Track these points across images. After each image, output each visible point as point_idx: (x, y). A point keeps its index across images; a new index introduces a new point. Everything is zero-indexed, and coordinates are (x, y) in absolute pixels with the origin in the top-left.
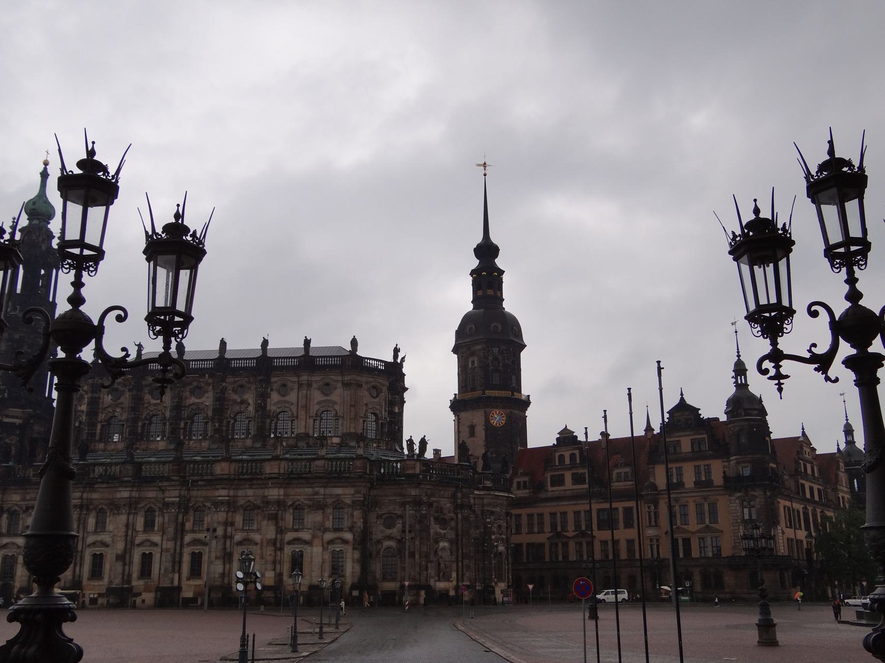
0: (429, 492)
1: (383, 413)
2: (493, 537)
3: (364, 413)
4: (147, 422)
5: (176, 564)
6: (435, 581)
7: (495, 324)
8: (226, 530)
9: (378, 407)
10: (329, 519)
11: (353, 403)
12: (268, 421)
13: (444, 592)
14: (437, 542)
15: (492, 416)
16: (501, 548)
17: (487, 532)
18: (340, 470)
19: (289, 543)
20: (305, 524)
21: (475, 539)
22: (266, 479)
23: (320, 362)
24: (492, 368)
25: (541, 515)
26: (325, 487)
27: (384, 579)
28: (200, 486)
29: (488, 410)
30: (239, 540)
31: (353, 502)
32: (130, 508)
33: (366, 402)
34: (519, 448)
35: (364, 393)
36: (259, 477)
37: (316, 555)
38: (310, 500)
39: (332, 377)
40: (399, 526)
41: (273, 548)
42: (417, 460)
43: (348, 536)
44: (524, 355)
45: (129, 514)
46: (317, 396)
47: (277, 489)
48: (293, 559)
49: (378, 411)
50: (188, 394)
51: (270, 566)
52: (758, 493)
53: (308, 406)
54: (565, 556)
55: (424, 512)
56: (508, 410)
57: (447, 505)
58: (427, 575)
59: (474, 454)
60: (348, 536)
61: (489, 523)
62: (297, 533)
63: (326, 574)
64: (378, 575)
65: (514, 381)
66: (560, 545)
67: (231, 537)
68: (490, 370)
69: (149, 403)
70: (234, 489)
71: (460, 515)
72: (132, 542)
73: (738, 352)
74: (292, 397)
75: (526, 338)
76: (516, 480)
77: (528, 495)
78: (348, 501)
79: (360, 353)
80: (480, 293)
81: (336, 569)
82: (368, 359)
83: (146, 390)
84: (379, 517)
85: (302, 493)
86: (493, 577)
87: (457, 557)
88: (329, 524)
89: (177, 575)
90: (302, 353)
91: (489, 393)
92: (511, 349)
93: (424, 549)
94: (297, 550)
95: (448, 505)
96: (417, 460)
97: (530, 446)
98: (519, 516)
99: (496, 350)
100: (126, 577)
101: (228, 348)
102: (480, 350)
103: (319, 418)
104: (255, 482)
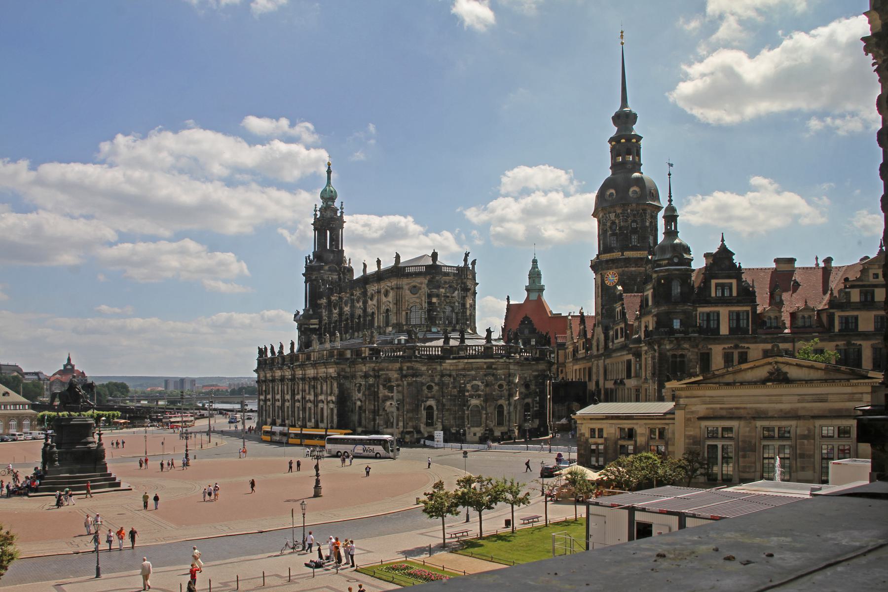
2: (467, 394)
5: (293, 412)
15: (606, 278)
17: (462, 391)
26: (326, 368)
29: (603, 272)
56: (621, 270)
57: (394, 375)
58: (375, 424)
60: (334, 398)
61: (463, 384)
67: (305, 398)
84: (356, 384)
85: (322, 371)
88: (329, 393)
95: (396, 376)
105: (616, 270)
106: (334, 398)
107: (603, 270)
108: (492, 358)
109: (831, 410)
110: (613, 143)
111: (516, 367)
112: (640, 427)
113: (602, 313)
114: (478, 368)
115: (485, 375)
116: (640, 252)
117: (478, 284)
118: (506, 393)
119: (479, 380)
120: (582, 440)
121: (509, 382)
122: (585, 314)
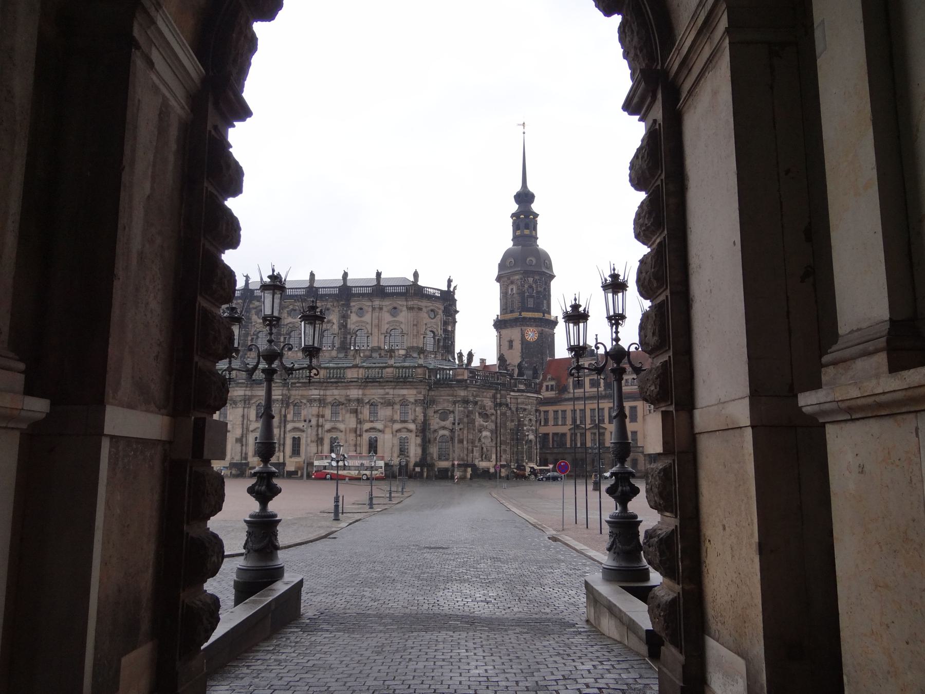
0: (475, 393)
1: (439, 330)
2: (525, 428)
3: (424, 330)
4: (255, 337)
6: (479, 461)
7: (531, 259)
8: (318, 421)
9: (435, 326)
10: (397, 412)
11: (415, 323)
12: (349, 337)
13: (486, 470)
14: (480, 431)
16: (531, 437)
17: (520, 424)
18: (405, 376)
19: (366, 431)
20: (379, 418)
21: (511, 430)
22: (348, 382)
23: (389, 290)
24: (527, 294)
25: (564, 412)
26: (394, 389)
27: (440, 459)
28: (300, 387)
30: (329, 428)
31: (416, 401)
32: (245, 403)
33: (425, 322)
34: (548, 358)
35: (424, 315)
36: (343, 380)
37: (387, 442)
38: (382, 398)
39: (399, 302)
40: (451, 419)
41: (355, 435)
42: (465, 369)
43: (412, 426)
44: (553, 283)
45: (244, 407)
46: (387, 317)
47: (357, 390)
48: (370, 444)
49: (436, 330)
50: (286, 314)
51: (353, 448)
53: (380, 325)
54: (584, 444)
55: (470, 409)
57: (488, 403)
58: (473, 456)
59: (513, 363)
61: (522, 417)
62: (372, 423)
63: (395, 455)
64: (435, 456)
65: (545, 305)
66: (579, 434)
67: (322, 426)
69: (256, 322)
70: (324, 390)
71: (499, 412)
72: (247, 429)
74: (367, 318)
75: (556, 270)
76: (545, 384)
77: (554, 396)
78: (412, 400)
79: (421, 283)
80: (518, 233)
81: (403, 451)
82: (427, 287)
83: (253, 311)
85: (375, 393)
86: (525, 458)
87: (496, 444)
88: (397, 417)
89: (282, 454)
90: (375, 283)
91: (524, 314)
93: (471, 437)
94: (373, 437)
95: (490, 403)
96: (465, 369)
97: (556, 358)
98: (546, 412)
99: (531, 280)
100: (243, 455)
101: (316, 278)
102: (518, 280)
103: (388, 335)
104: (340, 384)
106: (412, 426)
107: (522, 325)
110: (514, 218)
114: (532, 404)
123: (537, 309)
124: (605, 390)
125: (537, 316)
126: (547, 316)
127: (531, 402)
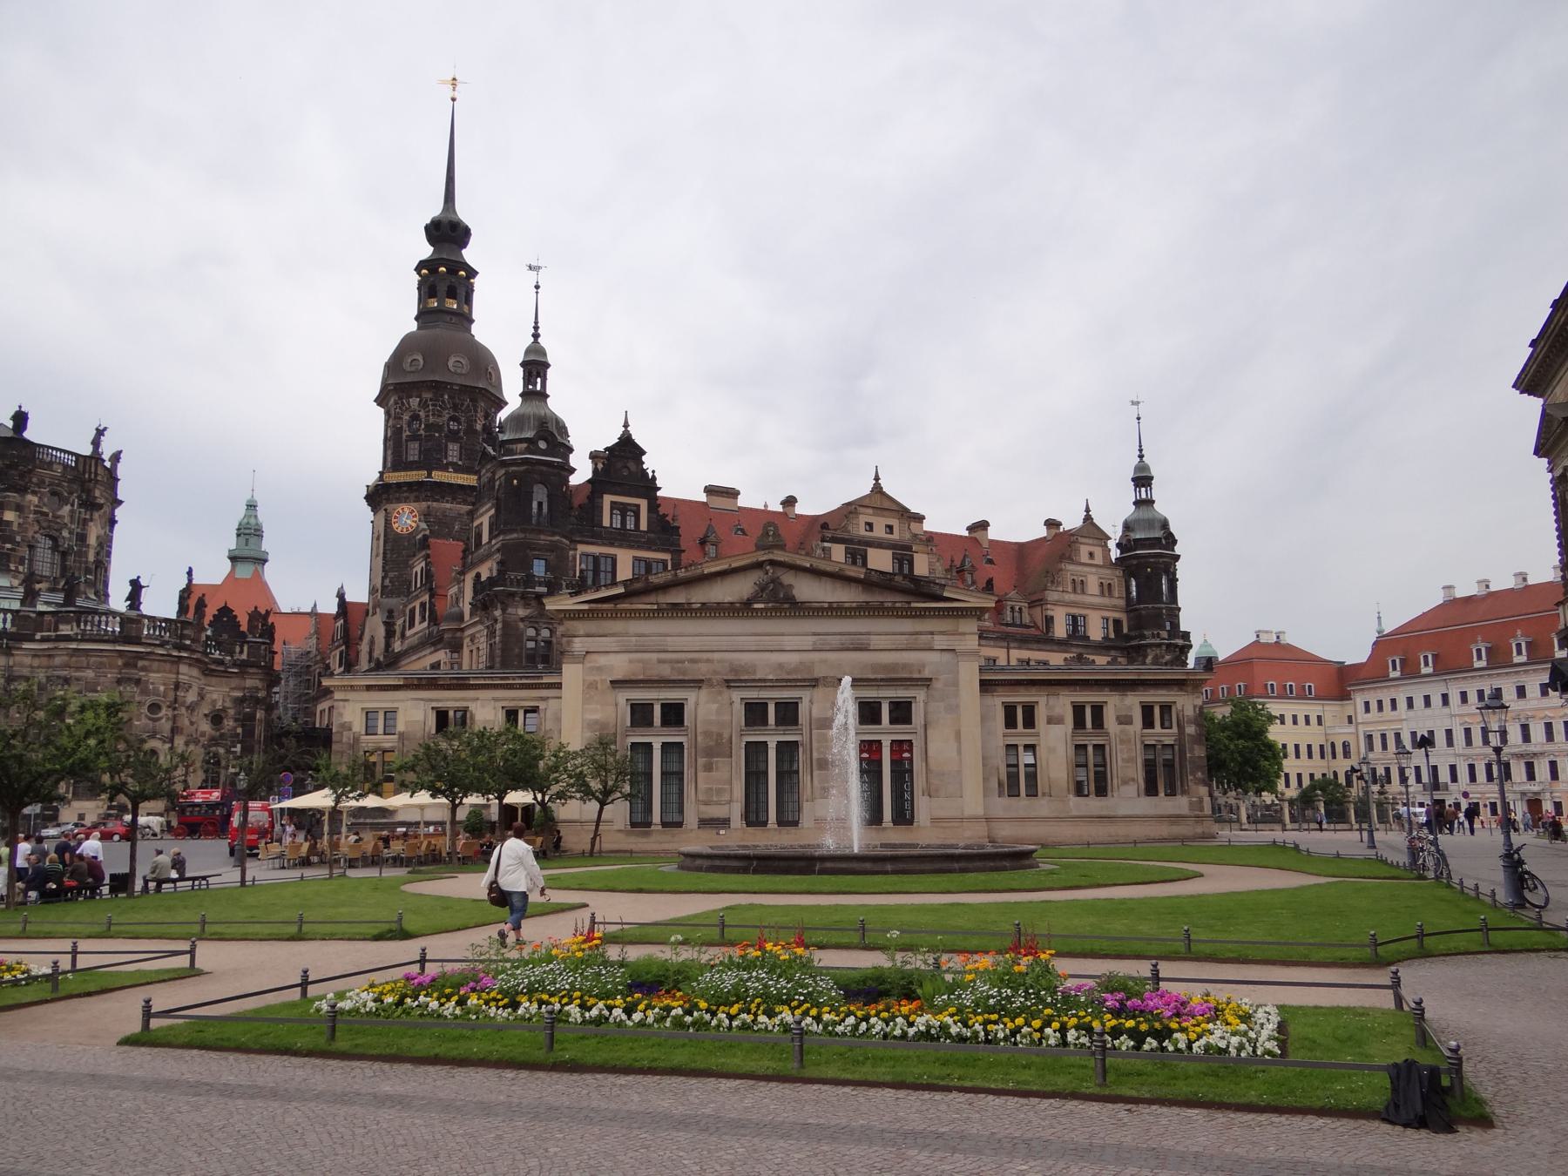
15: (396, 517)
24: (408, 433)
29: (389, 507)
52: (498, 613)
56: (424, 505)
68: (404, 437)
73: (536, 328)
92: (446, 397)
99: (414, 402)
105: (416, 504)
107: (389, 501)
108: (140, 644)
109: (875, 667)
111: (195, 672)
112: (483, 706)
113: (383, 587)
115: (119, 682)
116: (462, 475)
117: (121, 502)
118: (165, 726)
119: (103, 691)
120: (345, 740)
121: (176, 701)
122: (348, 598)
123: (431, 460)
124: (429, 627)
125: (415, 479)
126: (438, 476)
127: (101, 663)
